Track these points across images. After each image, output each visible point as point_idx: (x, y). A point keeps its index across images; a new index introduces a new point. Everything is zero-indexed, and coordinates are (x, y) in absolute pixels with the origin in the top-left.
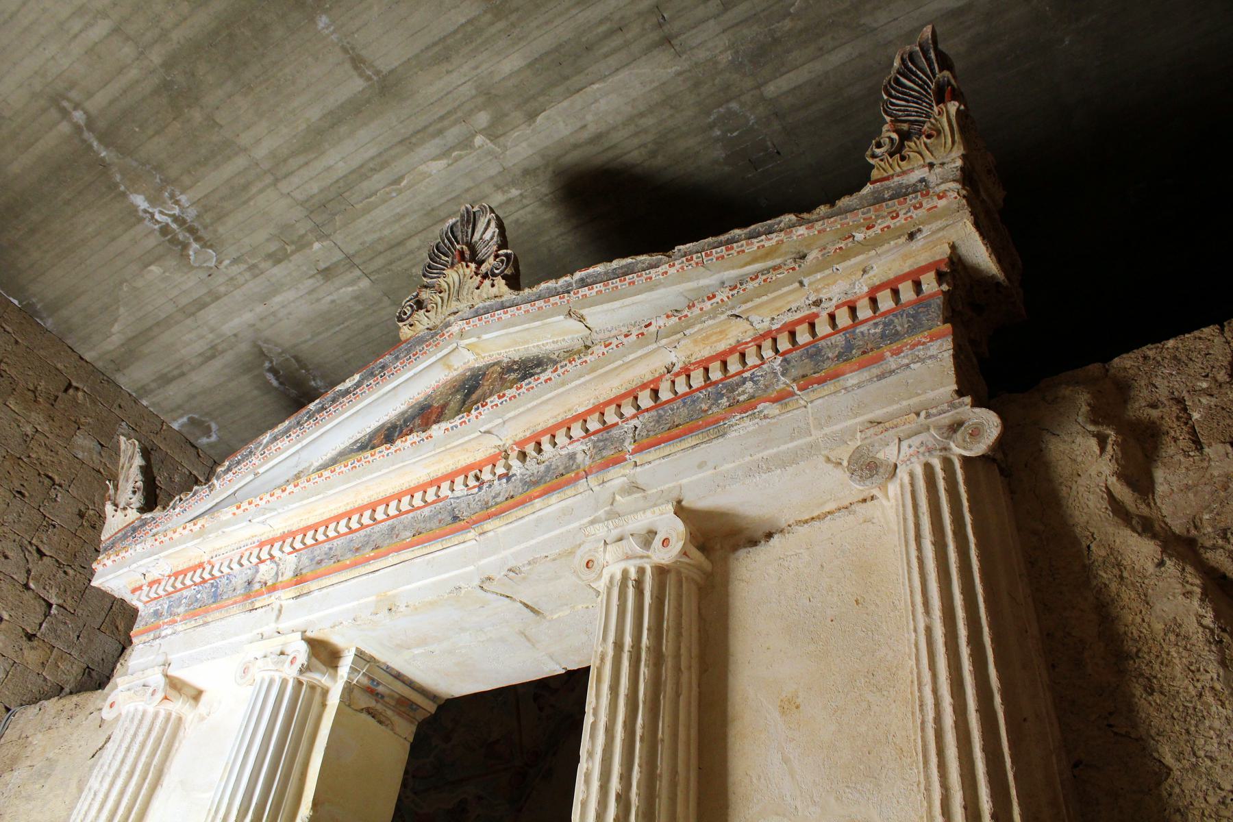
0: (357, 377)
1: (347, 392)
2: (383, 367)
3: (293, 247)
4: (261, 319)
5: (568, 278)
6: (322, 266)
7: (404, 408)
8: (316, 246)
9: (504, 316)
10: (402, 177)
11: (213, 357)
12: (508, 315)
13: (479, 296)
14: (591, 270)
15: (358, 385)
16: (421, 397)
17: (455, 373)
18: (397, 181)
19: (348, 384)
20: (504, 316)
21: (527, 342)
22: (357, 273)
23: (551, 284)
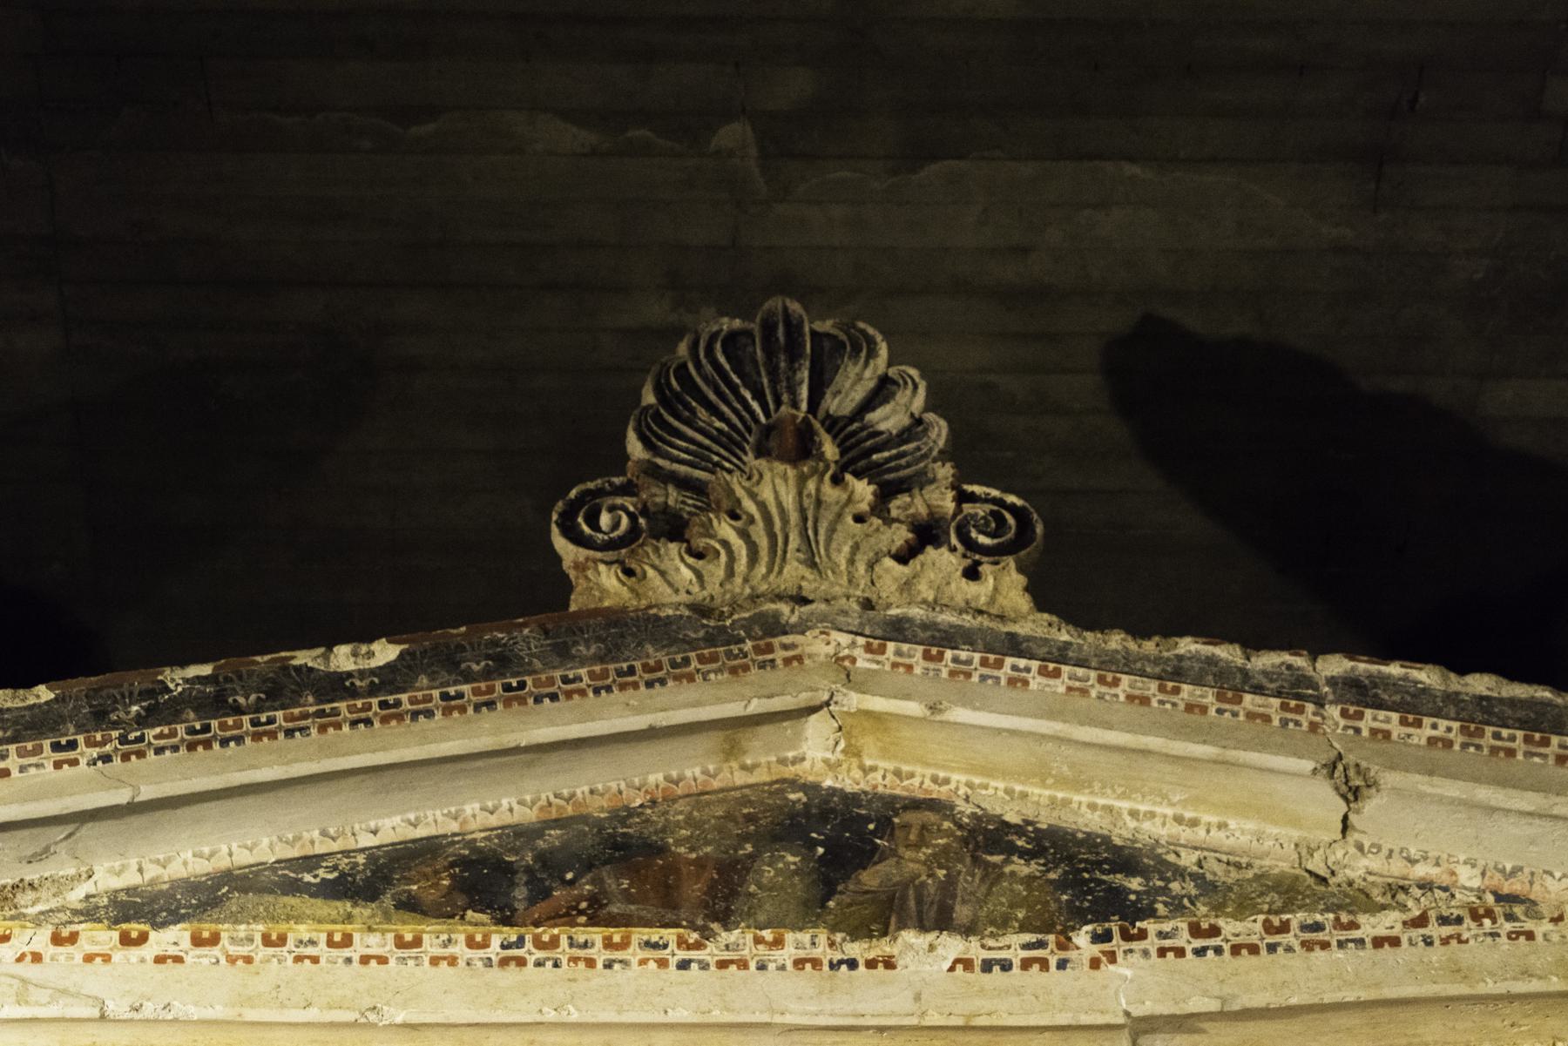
0: (385, 653)
1: (336, 686)
2: (503, 662)
5: (1300, 662)
7: (527, 815)
9: (1036, 682)
12: (1059, 686)
13: (907, 586)
14: (1394, 669)
15: (389, 680)
16: (598, 808)
17: (741, 778)
19: (343, 658)
20: (1036, 682)
21: (1078, 784)
23: (1228, 653)
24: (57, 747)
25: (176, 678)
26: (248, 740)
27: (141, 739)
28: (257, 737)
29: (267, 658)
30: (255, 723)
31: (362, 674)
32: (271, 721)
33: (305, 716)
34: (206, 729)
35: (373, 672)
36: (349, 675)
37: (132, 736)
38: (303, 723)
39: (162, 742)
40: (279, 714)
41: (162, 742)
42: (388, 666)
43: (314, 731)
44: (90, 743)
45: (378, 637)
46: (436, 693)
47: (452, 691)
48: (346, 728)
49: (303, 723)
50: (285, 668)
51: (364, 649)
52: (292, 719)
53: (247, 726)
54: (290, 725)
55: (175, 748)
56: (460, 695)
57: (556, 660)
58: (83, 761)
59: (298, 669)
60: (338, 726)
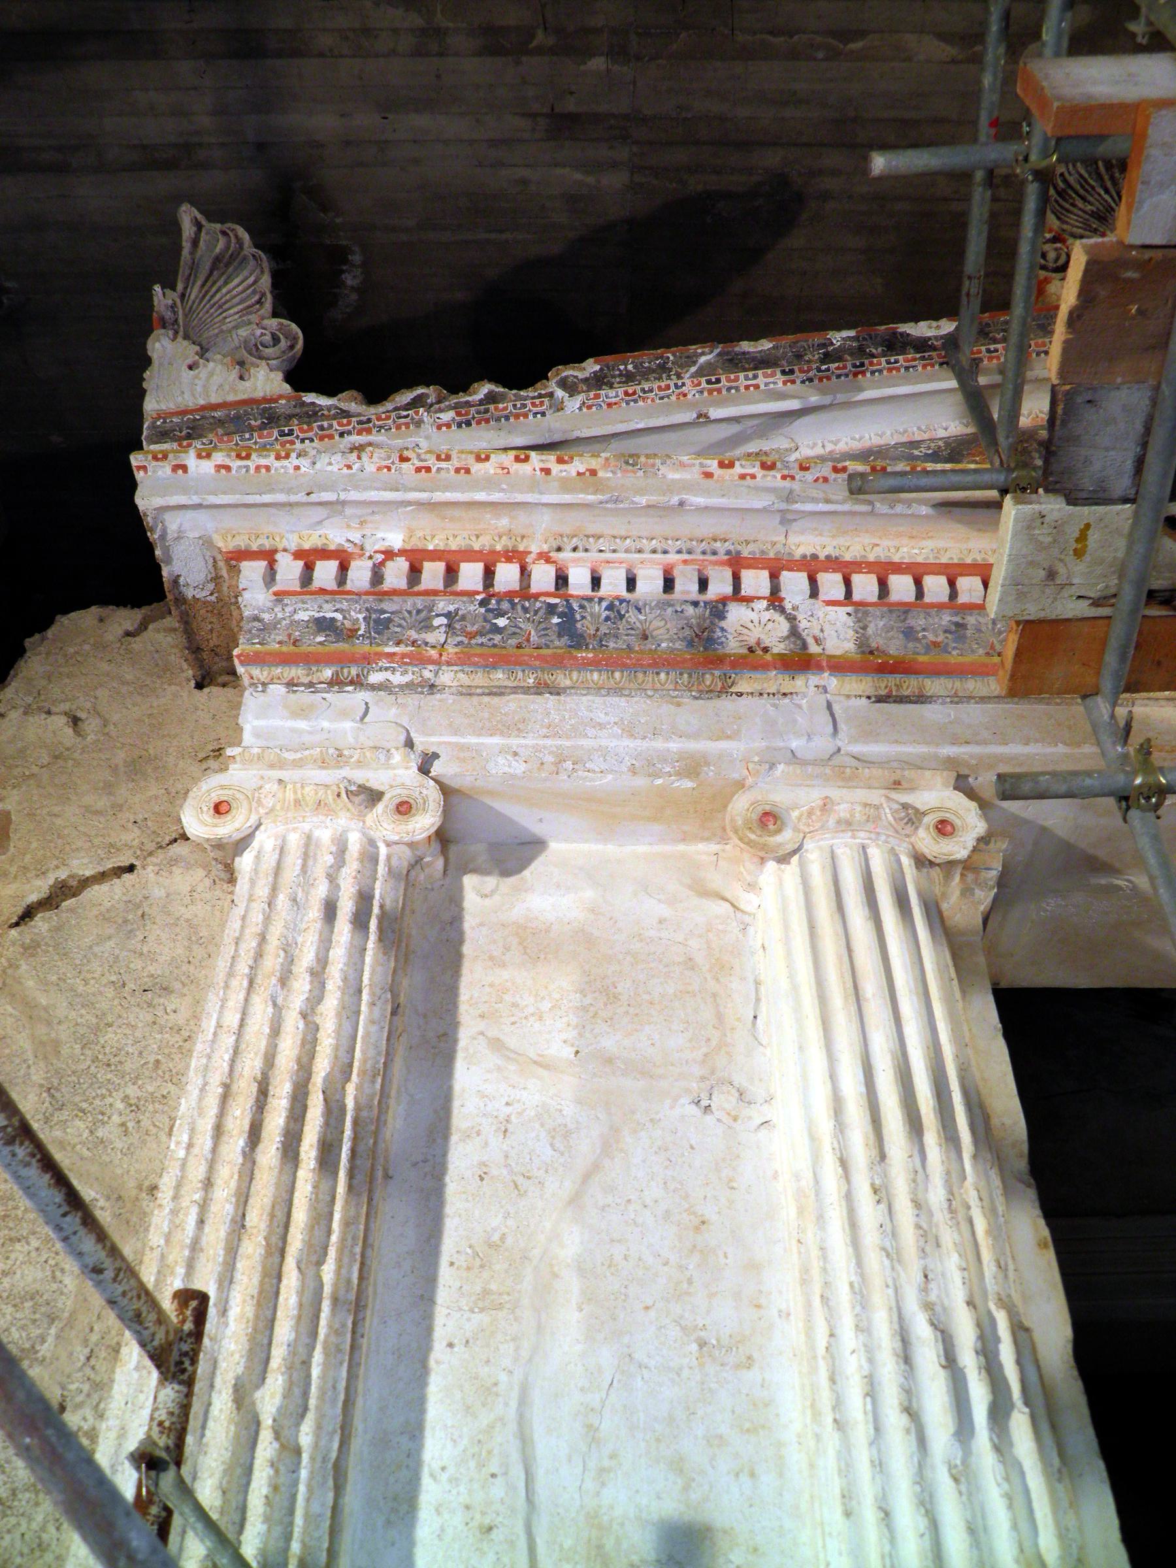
1: (922, 345)
3: (551, 41)
4: (348, 143)
6: (570, 105)
8: (598, 63)
10: (861, 34)
11: (170, 165)
18: (846, 35)
22: (623, 153)
24: (784, 373)
25: (838, 338)
26: (885, 372)
27: (828, 370)
28: (890, 370)
29: (883, 327)
30: (888, 362)
31: (936, 338)
32: (896, 362)
33: (914, 359)
34: (862, 365)
35: (942, 337)
36: (930, 338)
37: (823, 367)
38: (914, 363)
39: (839, 372)
40: (900, 358)
41: (839, 372)
42: (949, 334)
43: (920, 368)
44: (802, 371)
45: (941, 318)
46: (983, 348)
47: (992, 347)
48: (937, 367)
49: (914, 363)
50: (894, 333)
51: (934, 324)
52: (908, 361)
53: (884, 364)
54: (907, 364)
55: (847, 375)
56: (996, 350)
57: (1041, 334)
58: (798, 382)
59: (902, 334)
60: (932, 366)
